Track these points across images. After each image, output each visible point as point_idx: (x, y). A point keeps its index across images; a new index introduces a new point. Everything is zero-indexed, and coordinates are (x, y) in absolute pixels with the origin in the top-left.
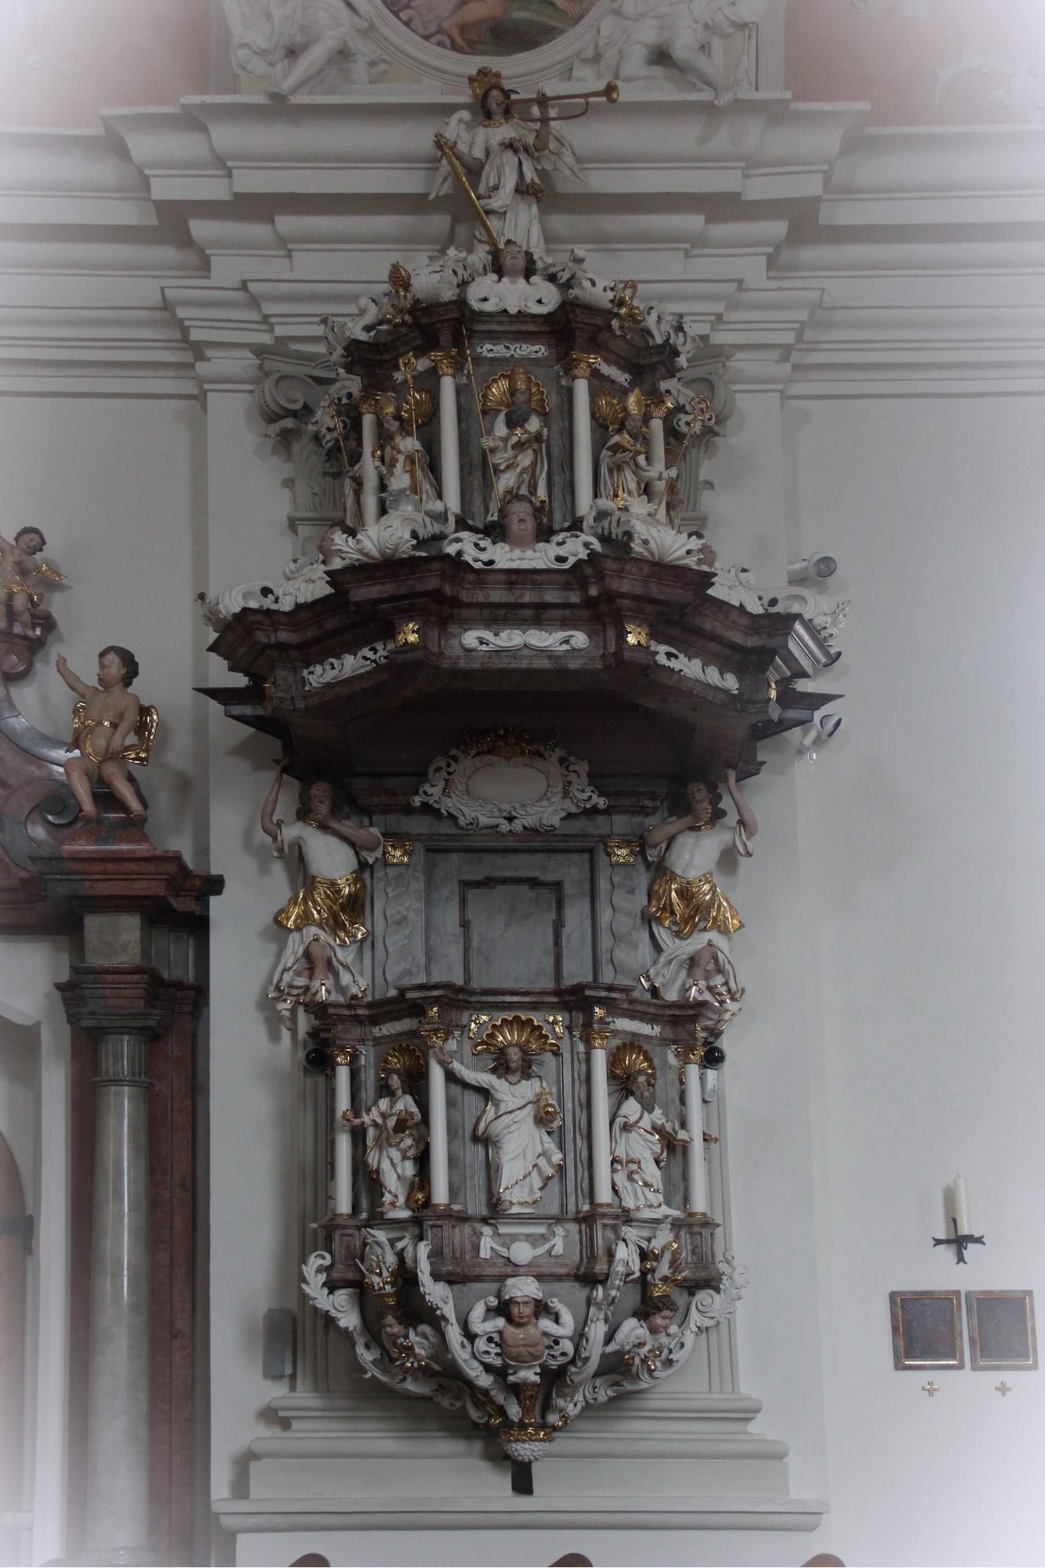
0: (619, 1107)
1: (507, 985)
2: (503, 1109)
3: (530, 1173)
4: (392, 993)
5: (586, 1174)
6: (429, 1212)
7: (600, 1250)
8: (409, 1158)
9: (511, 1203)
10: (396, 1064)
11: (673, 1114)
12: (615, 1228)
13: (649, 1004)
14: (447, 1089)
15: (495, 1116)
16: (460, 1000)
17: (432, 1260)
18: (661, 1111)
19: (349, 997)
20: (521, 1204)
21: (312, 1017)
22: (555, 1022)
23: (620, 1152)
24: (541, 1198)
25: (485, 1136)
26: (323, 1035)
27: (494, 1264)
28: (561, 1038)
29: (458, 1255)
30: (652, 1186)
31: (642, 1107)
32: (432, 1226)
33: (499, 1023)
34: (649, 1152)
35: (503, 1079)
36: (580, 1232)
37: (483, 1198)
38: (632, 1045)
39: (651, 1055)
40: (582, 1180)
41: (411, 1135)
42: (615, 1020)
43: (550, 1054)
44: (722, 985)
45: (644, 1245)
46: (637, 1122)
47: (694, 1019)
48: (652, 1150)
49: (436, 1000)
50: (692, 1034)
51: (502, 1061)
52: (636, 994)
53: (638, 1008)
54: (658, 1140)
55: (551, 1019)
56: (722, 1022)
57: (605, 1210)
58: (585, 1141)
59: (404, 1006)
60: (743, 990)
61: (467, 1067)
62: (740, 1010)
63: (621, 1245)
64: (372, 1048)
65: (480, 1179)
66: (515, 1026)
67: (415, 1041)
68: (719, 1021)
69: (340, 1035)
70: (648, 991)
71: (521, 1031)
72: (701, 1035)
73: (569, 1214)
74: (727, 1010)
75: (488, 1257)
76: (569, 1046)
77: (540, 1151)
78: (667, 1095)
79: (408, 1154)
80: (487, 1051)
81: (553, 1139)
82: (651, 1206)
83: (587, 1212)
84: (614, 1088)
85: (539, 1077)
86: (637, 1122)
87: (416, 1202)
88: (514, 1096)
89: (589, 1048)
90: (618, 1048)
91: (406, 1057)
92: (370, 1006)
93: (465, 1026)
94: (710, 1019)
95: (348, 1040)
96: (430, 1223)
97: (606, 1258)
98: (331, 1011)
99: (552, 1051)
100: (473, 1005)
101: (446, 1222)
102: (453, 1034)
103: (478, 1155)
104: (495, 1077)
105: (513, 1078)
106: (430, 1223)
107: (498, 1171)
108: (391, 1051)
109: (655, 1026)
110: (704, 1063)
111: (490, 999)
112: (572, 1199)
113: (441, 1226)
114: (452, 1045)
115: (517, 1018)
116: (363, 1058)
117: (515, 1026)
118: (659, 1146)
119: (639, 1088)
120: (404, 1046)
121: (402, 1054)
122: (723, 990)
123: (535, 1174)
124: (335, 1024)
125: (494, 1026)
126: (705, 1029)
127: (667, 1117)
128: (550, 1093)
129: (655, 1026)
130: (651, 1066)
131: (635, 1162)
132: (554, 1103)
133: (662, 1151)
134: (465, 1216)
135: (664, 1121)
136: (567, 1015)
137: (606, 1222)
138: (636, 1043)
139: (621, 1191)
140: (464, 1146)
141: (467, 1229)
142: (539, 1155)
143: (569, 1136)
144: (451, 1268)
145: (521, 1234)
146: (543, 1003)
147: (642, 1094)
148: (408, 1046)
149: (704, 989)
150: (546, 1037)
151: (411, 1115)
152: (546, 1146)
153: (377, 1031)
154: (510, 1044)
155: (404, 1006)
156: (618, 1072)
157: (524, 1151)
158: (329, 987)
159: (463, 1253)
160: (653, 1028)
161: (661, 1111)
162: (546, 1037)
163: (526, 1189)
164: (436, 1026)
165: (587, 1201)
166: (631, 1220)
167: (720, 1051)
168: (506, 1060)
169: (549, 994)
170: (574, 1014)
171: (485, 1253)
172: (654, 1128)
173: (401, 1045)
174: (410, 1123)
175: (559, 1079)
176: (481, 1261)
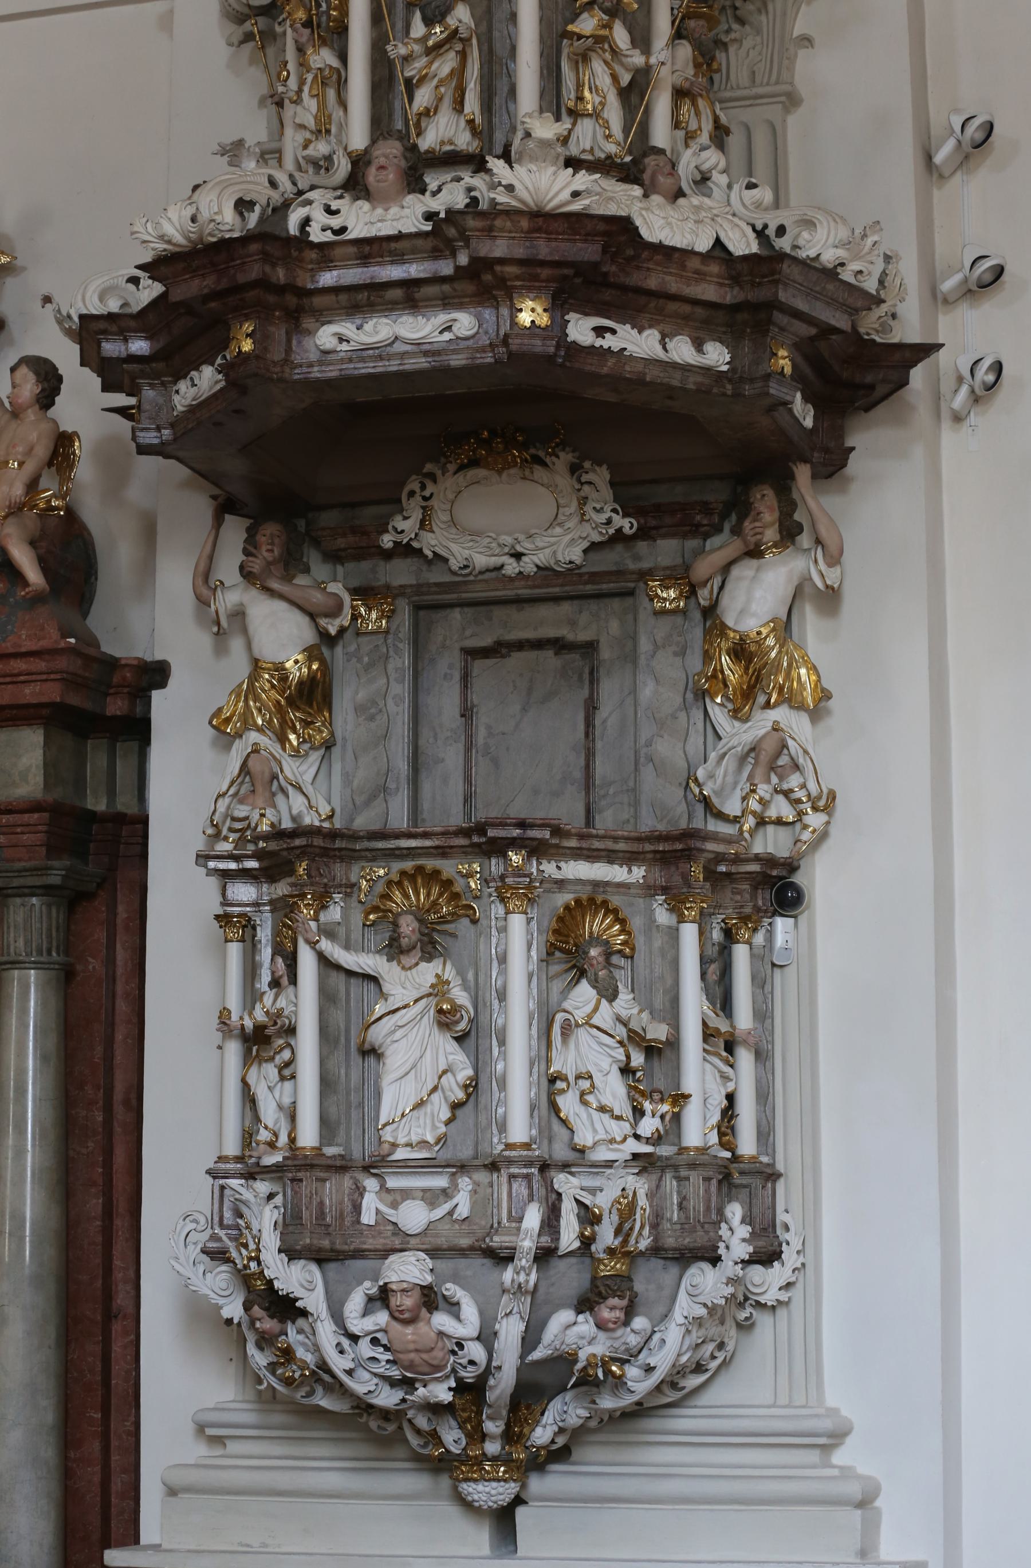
27: (380, 1233)
75: (372, 1223)
105: (408, 960)
111: (380, 845)
145: (417, 1189)
152: (451, 1058)
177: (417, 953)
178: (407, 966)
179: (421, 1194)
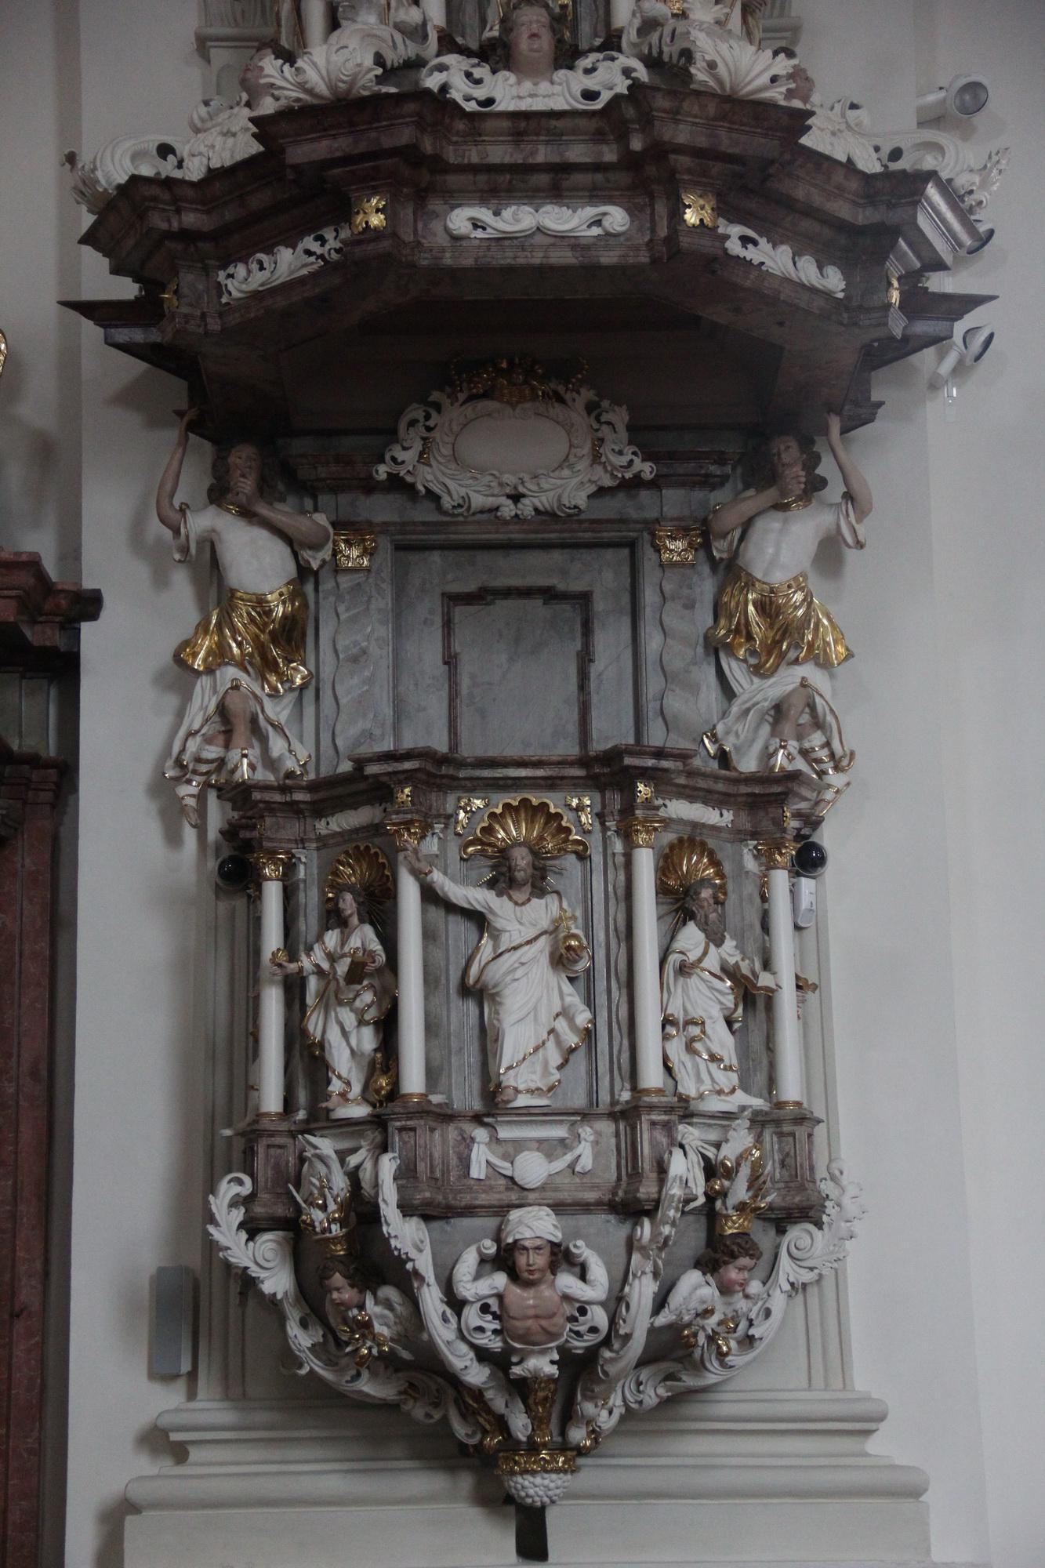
0: (673, 938)
1: (512, 751)
2: (505, 942)
3: (544, 1043)
4: (346, 766)
5: (626, 1042)
6: (396, 1107)
7: (646, 1164)
8: (367, 1023)
9: (517, 1091)
10: (349, 876)
11: (752, 947)
12: (668, 1127)
13: (716, 778)
14: (424, 912)
15: (492, 956)
16: (443, 777)
17: (400, 1182)
18: (734, 943)
19: (282, 775)
20: (531, 1092)
21: (229, 805)
22: (580, 808)
23: (675, 1009)
24: (559, 1081)
25: (478, 986)
26: (244, 834)
27: (491, 1188)
28: (589, 832)
29: (438, 1174)
30: (721, 1060)
31: (707, 937)
32: (401, 1130)
33: (499, 811)
34: (718, 1007)
35: (505, 898)
36: (617, 1135)
37: (476, 1083)
38: (691, 840)
39: (719, 856)
40: (620, 1051)
41: (371, 986)
42: (667, 802)
43: (572, 858)
44: (822, 747)
45: (711, 1153)
46: (700, 960)
47: (781, 799)
48: (721, 1003)
49: (408, 777)
50: (779, 823)
51: (504, 869)
52: (697, 762)
53: (702, 783)
54: (731, 988)
55: (575, 802)
56: (822, 804)
57: (654, 1099)
58: (624, 991)
59: (362, 786)
60: (852, 754)
61: (453, 879)
62: (848, 784)
63: (677, 1153)
64: (315, 854)
65: (471, 1056)
66: (523, 815)
67: (377, 840)
68: (817, 803)
69: (269, 833)
70: (714, 758)
71: (531, 822)
72: (793, 824)
73: (601, 1105)
74: (829, 786)
75: (482, 1177)
76: (600, 843)
77: (557, 1008)
78: (743, 919)
79: (367, 1017)
80: (482, 853)
81: (576, 990)
82: (720, 1092)
83: (627, 1102)
84: (665, 908)
85: (558, 893)
86: (700, 960)
87: (378, 1092)
88: (521, 923)
89: (630, 846)
90: (672, 847)
91: (365, 866)
92: (312, 787)
93: (451, 816)
94: (806, 799)
95: (280, 841)
96: (398, 1124)
97: (654, 1175)
98: (257, 795)
99: (576, 853)
100: (463, 783)
101: (422, 1122)
102: (432, 828)
103: (468, 1016)
104: (493, 893)
106: (398, 1124)
107: (496, 1040)
108: (342, 857)
109: (725, 812)
110: (797, 868)
111: (486, 773)
112: (605, 1083)
113: (413, 1129)
114: (431, 845)
115: (525, 802)
116: (302, 868)
117: (523, 815)
118: (731, 997)
119: (702, 907)
120: (362, 848)
121: (357, 860)
122: (823, 754)
123: (551, 1044)
124: (262, 817)
125: (492, 815)
126: (798, 815)
127: (743, 952)
128: (574, 918)
129: (725, 812)
130: (720, 874)
131: (696, 1024)
132: (579, 932)
133: (736, 1005)
134: (449, 1112)
135: (738, 958)
136: (598, 796)
137: (654, 1117)
138: (698, 839)
139: (676, 1069)
140: (448, 1002)
141: (452, 1132)
142: (557, 1015)
143: (601, 985)
144: (428, 1195)
145: (531, 1140)
146: (563, 778)
147: (706, 916)
148: (367, 848)
149: (795, 752)
150: (568, 831)
151: (371, 954)
152: (568, 999)
153: (322, 827)
154: (516, 843)
155: (362, 786)
156: (671, 882)
157: (535, 1008)
158: (254, 761)
159: (446, 1171)
160: (721, 815)
161: (734, 943)
162: (568, 831)
163: (539, 1068)
164: (409, 816)
165: (627, 1086)
166: (692, 1115)
167: (819, 849)
168: (510, 868)
169: (572, 764)
170: (608, 794)
171: (477, 1171)
172: (723, 969)
173: (357, 847)
174: (370, 968)
175: (585, 896)
176: (472, 1182)
177: (528, 889)
178: (520, 902)
179: (536, 1145)
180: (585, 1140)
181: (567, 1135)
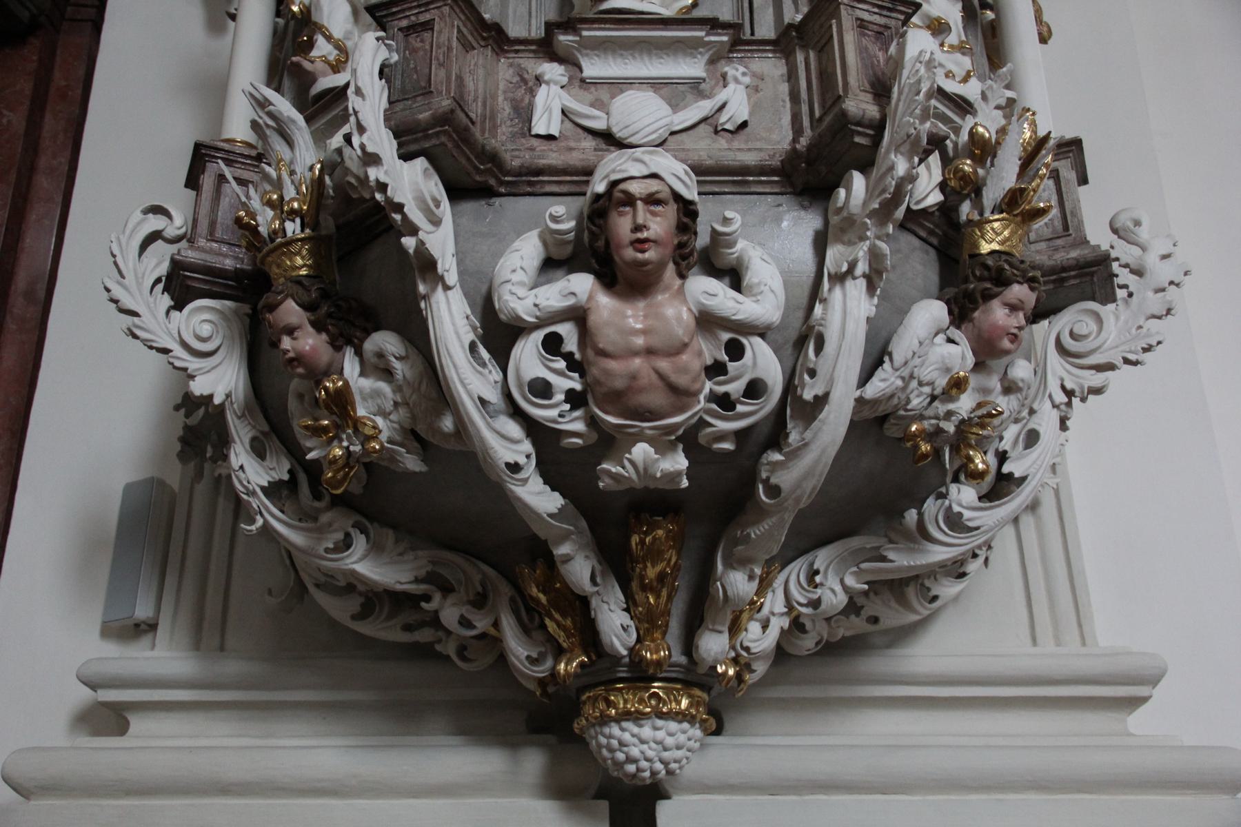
171: (545, 121)
180: (737, 81)
181: (704, 75)
